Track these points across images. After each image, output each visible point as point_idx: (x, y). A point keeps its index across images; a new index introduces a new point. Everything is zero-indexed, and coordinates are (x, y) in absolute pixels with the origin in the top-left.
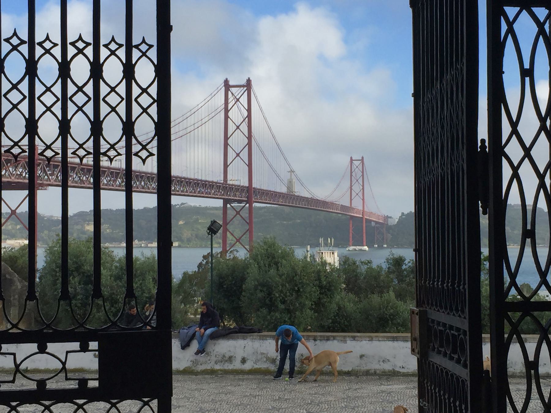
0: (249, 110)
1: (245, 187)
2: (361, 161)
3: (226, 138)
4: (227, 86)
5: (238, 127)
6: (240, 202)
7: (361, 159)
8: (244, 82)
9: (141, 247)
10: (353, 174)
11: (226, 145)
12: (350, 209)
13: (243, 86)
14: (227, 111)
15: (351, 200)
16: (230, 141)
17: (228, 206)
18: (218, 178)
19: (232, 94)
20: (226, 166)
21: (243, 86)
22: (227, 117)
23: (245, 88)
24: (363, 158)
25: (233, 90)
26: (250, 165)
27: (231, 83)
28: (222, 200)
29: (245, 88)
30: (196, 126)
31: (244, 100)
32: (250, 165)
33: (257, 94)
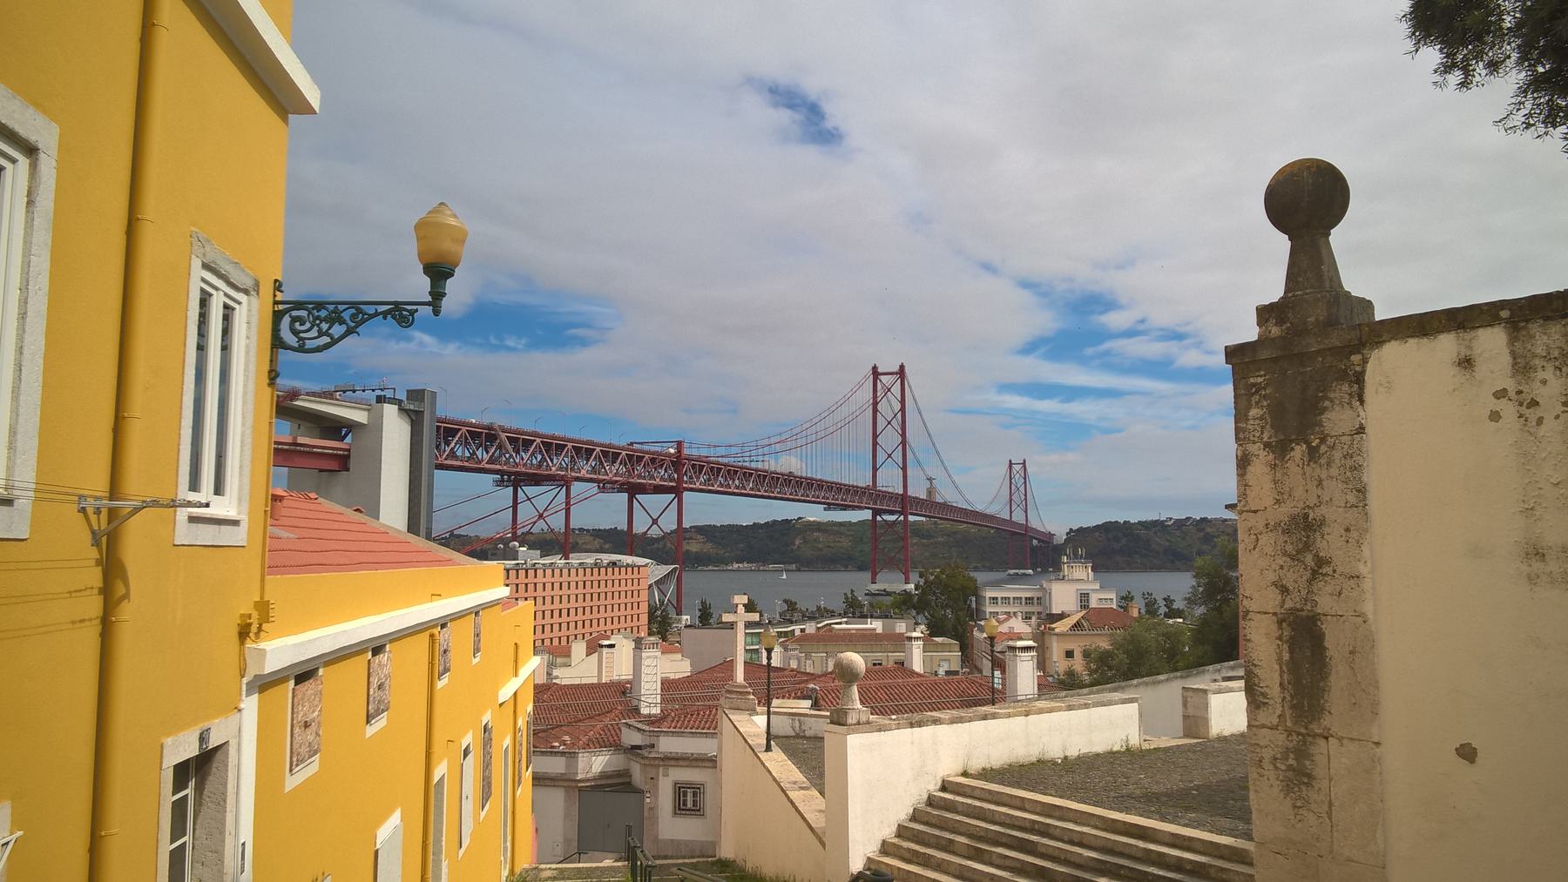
0: (903, 401)
3: (875, 436)
4: (876, 373)
5: (889, 423)
6: (892, 513)
8: (896, 369)
9: (751, 570)
11: (875, 444)
12: (1010, 522)
13: (896, 373)
14: (875, 404)
15: (1011, 512)
17: (879, 518)
18: (864, 480)
21: (896, 373)
22: (875, 411)
25: (882, 377)
26: (904, 469)
27: (880, 370)
28: (871, 511)
30: (823, 416)
31: (896, 389)
32: (904, 469)
33: (911, 383)
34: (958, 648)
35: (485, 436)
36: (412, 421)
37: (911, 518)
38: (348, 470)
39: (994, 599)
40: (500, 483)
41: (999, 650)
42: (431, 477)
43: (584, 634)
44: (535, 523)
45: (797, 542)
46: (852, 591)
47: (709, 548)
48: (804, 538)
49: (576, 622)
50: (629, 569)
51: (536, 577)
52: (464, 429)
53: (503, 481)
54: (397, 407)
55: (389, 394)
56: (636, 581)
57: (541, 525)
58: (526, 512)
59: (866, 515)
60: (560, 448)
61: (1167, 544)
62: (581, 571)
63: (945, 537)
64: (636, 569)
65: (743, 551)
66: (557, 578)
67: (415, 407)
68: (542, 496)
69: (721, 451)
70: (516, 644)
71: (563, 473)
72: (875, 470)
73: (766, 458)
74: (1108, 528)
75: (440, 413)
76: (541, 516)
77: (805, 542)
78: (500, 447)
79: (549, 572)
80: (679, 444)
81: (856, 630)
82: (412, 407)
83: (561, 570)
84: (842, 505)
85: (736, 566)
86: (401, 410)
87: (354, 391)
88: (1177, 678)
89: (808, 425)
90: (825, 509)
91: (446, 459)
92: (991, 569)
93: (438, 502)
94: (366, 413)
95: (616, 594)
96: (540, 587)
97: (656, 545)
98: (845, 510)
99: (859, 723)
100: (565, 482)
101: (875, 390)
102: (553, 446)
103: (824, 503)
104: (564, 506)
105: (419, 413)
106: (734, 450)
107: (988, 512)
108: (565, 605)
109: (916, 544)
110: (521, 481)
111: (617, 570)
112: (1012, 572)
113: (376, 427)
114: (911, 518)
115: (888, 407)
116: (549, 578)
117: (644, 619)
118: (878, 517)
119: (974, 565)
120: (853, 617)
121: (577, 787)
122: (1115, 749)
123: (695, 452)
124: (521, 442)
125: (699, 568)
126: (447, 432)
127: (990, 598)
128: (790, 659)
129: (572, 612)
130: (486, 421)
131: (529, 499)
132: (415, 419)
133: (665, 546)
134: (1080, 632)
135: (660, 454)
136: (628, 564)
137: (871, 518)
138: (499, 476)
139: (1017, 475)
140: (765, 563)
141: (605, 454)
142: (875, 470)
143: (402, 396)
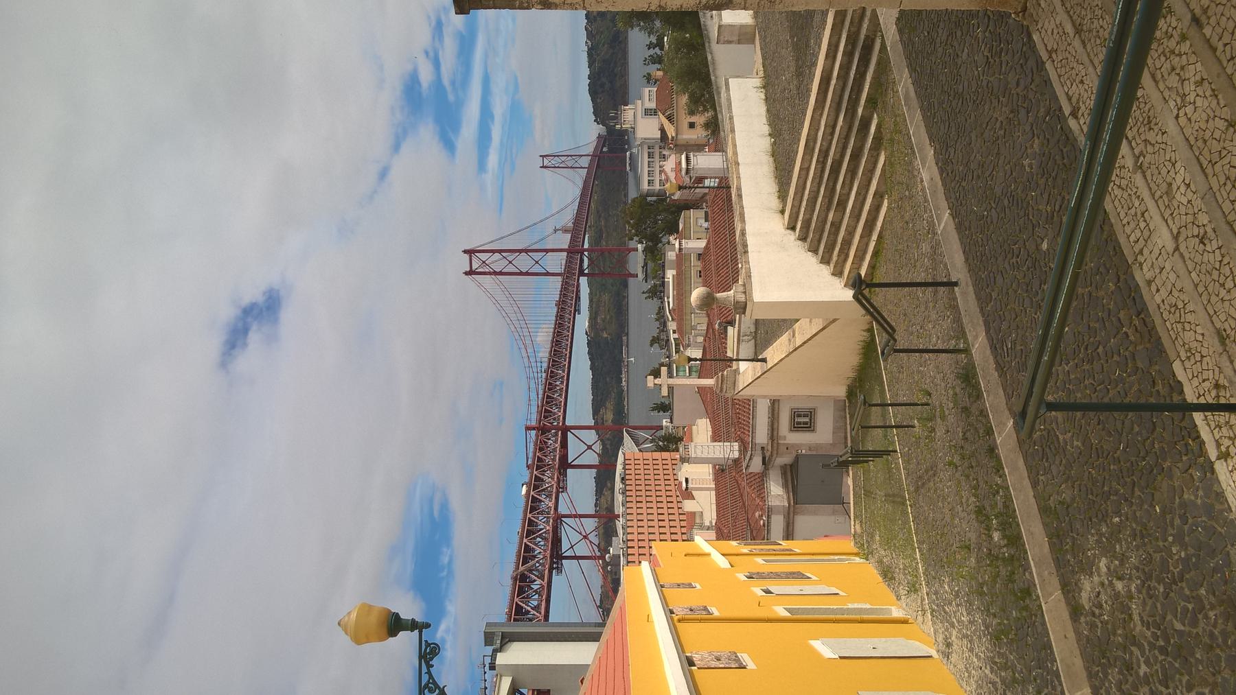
0: (493, 251)
3: (521, 274)
4: (470, 273)
5: (510, 262)
6: (582, 261)
8: (467, 256)
11: (527, 274)
13: (471, 256)
14: (495, 273)
17: (586, 272)
21: (471, 256)
22: (501, 273)
24: (541, 156)
25: (474, 268)
26: (547, 251)
27: (468, 269)
30: (505, 315)
31: (483, 256)
32: (547, 251)
34: (687, 212)
35: (522, 583)
36: (509, 641)
37: (586, 246)
38: (549, 691)
39: (649, 183)
40: (559, 570)
41: (689, 180)
42: (554, 625)
43: (678, 502)
44: (591, 542)
45: (605, 335)
46: (643, 293)
47: (610, 405)
48: (602, 330)
49: (668, 508)
50: (627, 467)
51: (633, 540)
52: (516, 600)
53: (557, 568)
54: (498, 654)
55: (488, 660)
56: (636, 462)
57: (592, 537)
58: (583, 549)
59: (584, 281)
60: (531, 523)
61: (606, 46)
62: (629, 505)
63: (601, 219)
64: (627, 462)
65: (612, 378)
66: (635, 523)
67: (498, 639)
68: (569, 536)
69: (533, 395)
70: (685, 555)
71: (551, 521)
72: (548, 274)
73: (538, 360)
74: (594, 91)
75: (503, 618)
76: (585, 537)
77: (605, 329)
78: (531, 571)
79: (629, 530)
80: (528, 428)
81: (673, 290)
82: (499, 642)
83: (628, 520)
84: (576, 300)
85: (624, 384)
86: (500, 649)
87: (486, 688)
88: (710, 46)
90: (579, 314)
91: (540, 614)
92: (626, 184)
93: (575, 619)
94: (503, 678)
95: (647, 477)
96: (641, 537)
97: (608, 446)
98: (580, 298)
99: (745, 293)
100: (559, 518)
102: (530, 529)
103: (575, 315)
104: (577, 519)
105: (504, 636)
106: (533, 385)
107: (581, 185)
108: (655, 517)
109: (606, 243)
110: (557, 552)
111: (627, 477)
112: (628, 168)
113: (515, 670)
114: (586, 246)
115: (497, 263)
116: (634, 530)
117: (666, 455)
120: (664, 292)
121: (794, 506)
122: (764, 97)
123: (534, 416)
124: (526, 554)
125: (626, 412)
126: (518, 613)
127: (649, 186)
128: (696, 342)
129: (660, 511)
130: (509, 582)
131: (572, 547)
132: (508, 639)
133: (608, 439)
134: (675, 116)
135: (536, 444)
136: (623, 468)
137: (586, 278)
138: (554, 571)
139: (551, 161)
140: (621, 360)
141: (536, 487)
142: (548, 274)
143: (489, 650)
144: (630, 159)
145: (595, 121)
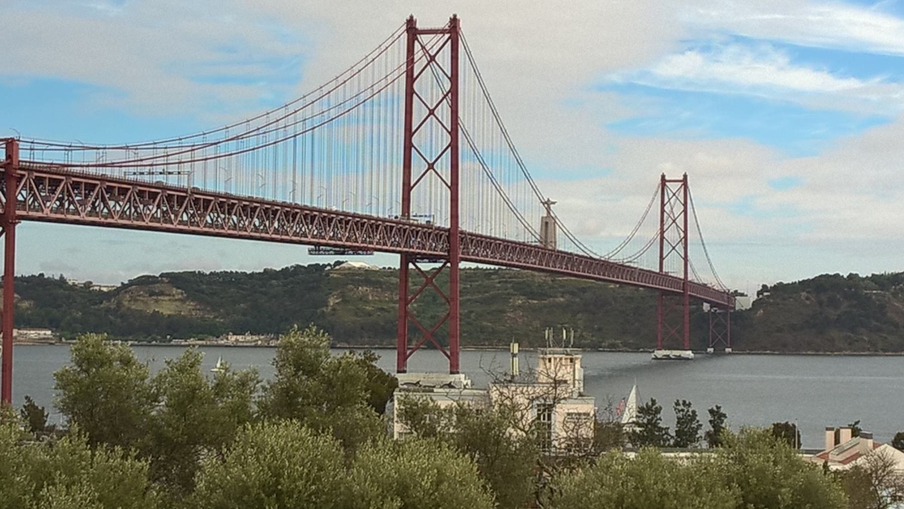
1: (445, 230)
2: (680, 184)
3: (409, 133)
4: (412, 30)
6: (433, 259)
7: (681, 178)
8: (444, 23)
10: (667, 208)
11: (408, 146)
13: (443, 32)
14: (411, 79)
16: (415, 140)
17: (411, 266)
19: (423, 47)
20: (407, 188)
21: (443, 32)
22: (410, 93)
23: (447, 36)
24: (685, 176)
25: (424, 38)
26: (454, 187)
27: (419, 26)
28: (399, 256)
29: (447, 36)
31: (444, 59)
32: (454, 187)
37: (463, 265)
45: (332, 302)
47: (188, 309)
48: (342, 295)
59: (393, 261)
63: (567, 296)
65: (244, 315)
73: (186, 167)
77: (345, 301)
84: (335, 246)
85: (232, 338)
89: (282, 113)
90: (311, 252)
97: (105, 304)
101: (410, 62)
107: (618, 258)
109: (519, 306)
112: (660, 353)
114: (463, 265)
118: (411, 266)
119: (612, 341)
125: (174, 342)
133: (119, 304)
137: (398, 267)
142: (407, 188)
144: (679, 358)
145: (764, 286)
